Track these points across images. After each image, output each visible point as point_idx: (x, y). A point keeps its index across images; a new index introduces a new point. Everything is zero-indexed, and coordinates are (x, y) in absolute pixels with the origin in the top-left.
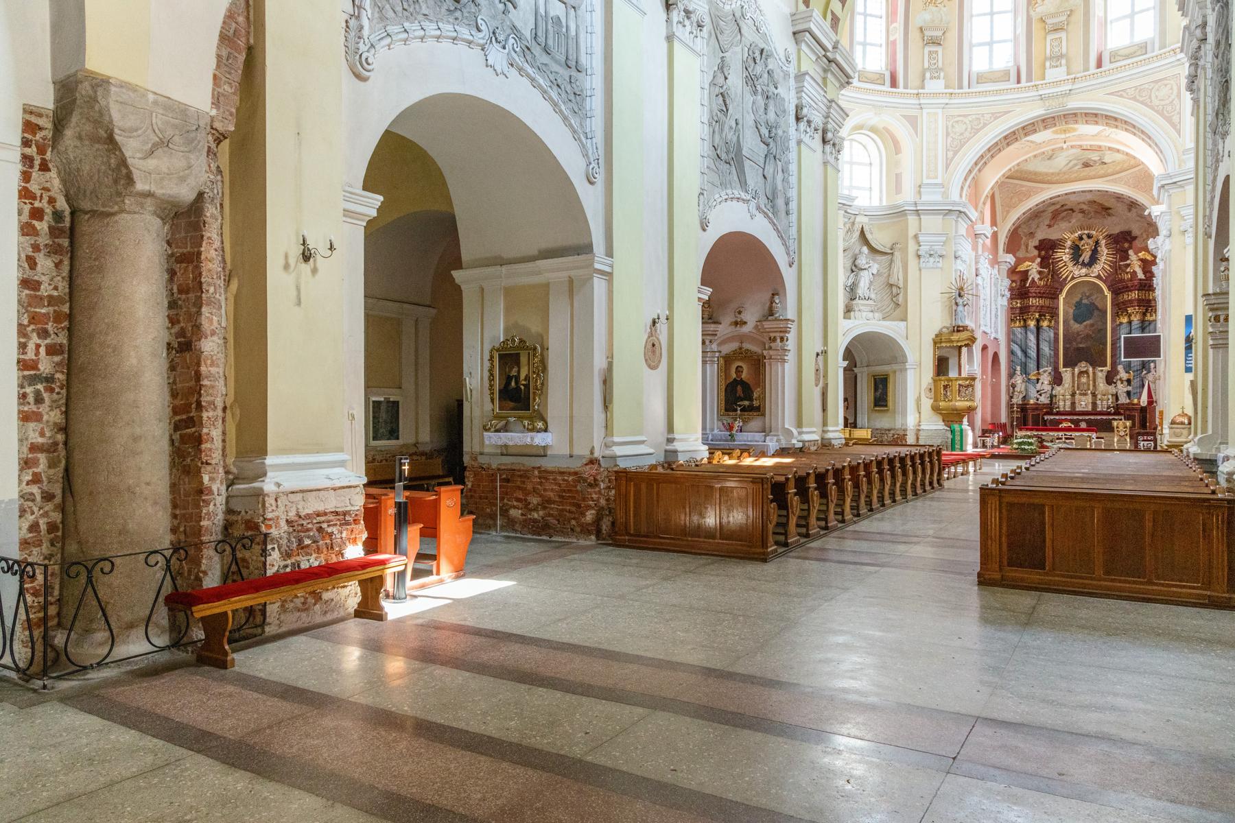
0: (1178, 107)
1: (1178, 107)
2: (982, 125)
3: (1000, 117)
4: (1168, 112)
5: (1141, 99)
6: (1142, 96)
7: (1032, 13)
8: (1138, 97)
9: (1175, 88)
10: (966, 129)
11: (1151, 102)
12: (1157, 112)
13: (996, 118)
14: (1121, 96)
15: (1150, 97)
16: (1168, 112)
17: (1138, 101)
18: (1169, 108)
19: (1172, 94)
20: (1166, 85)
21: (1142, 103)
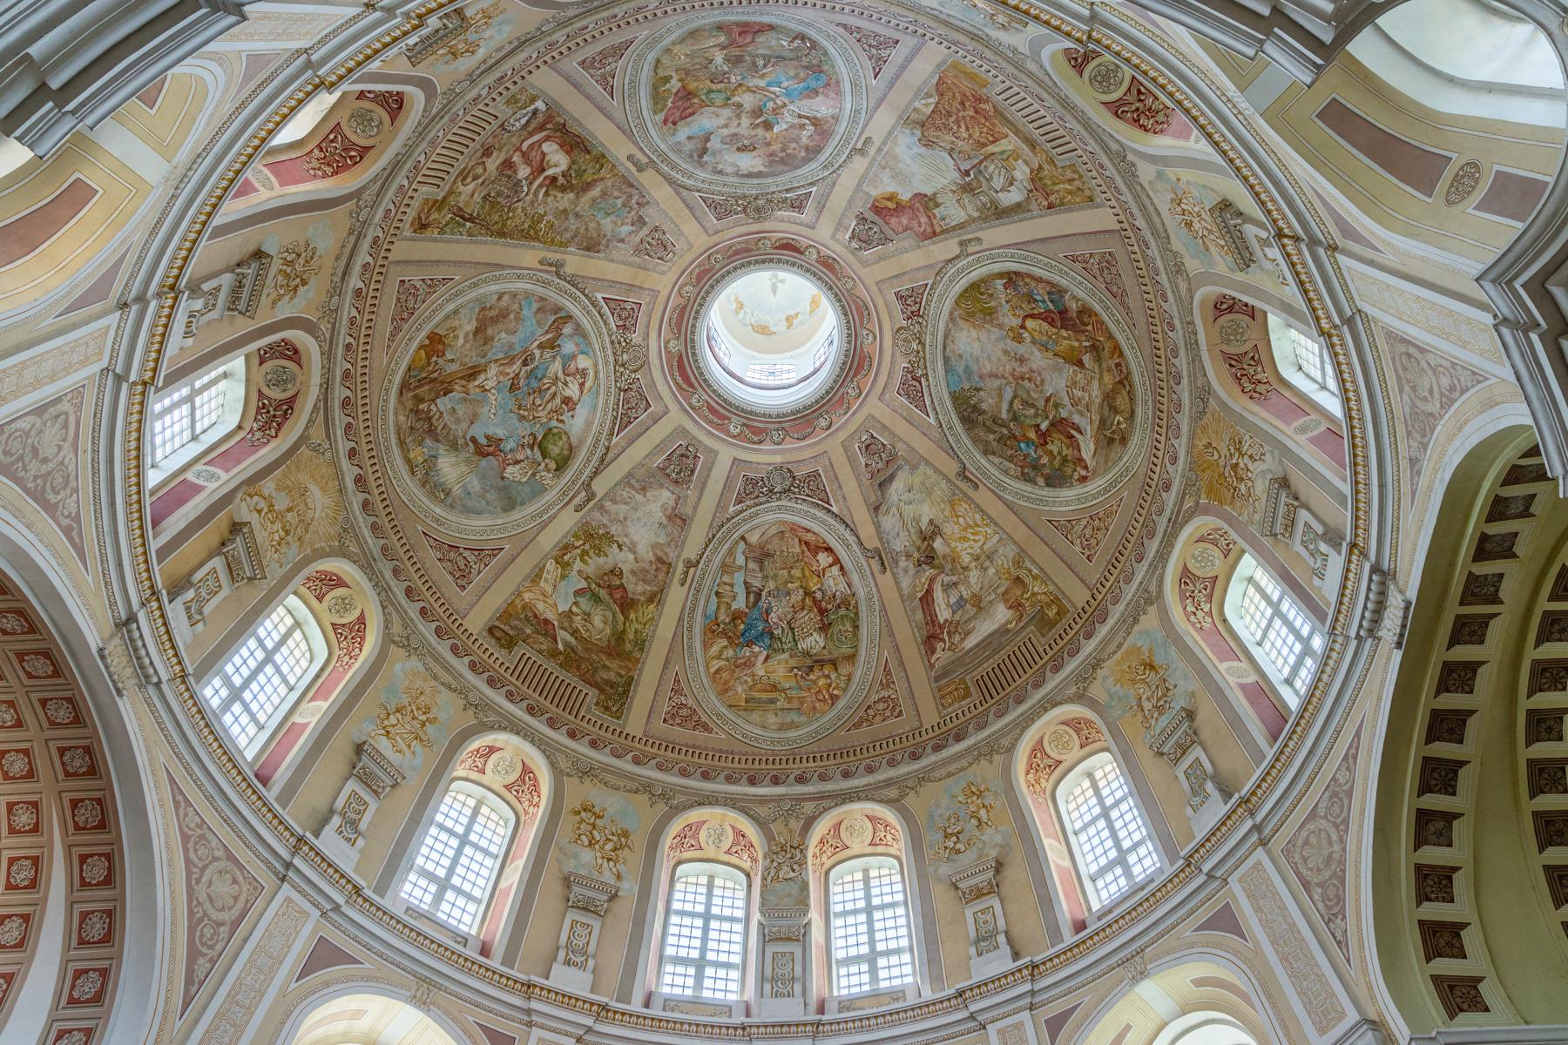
0: (219, 947)
1: (219, 947)
2: (52, 498)
3: (71, 540)
4: (202, 935)
5: (192, 855)
6: (196, 851)
7: (239, 495)
8: (191, 844)
9: (240, 904)
10: (45, 460)
11: (197, 883)
12: (191, 913)
13: (67, 531)
14: (177, 804)
15: (203, 870)
16: (202, 935)
17: (186, 851)
18: (208, 932)
19: (230, 908)
20: (235, 881)
21: (188, 862)
